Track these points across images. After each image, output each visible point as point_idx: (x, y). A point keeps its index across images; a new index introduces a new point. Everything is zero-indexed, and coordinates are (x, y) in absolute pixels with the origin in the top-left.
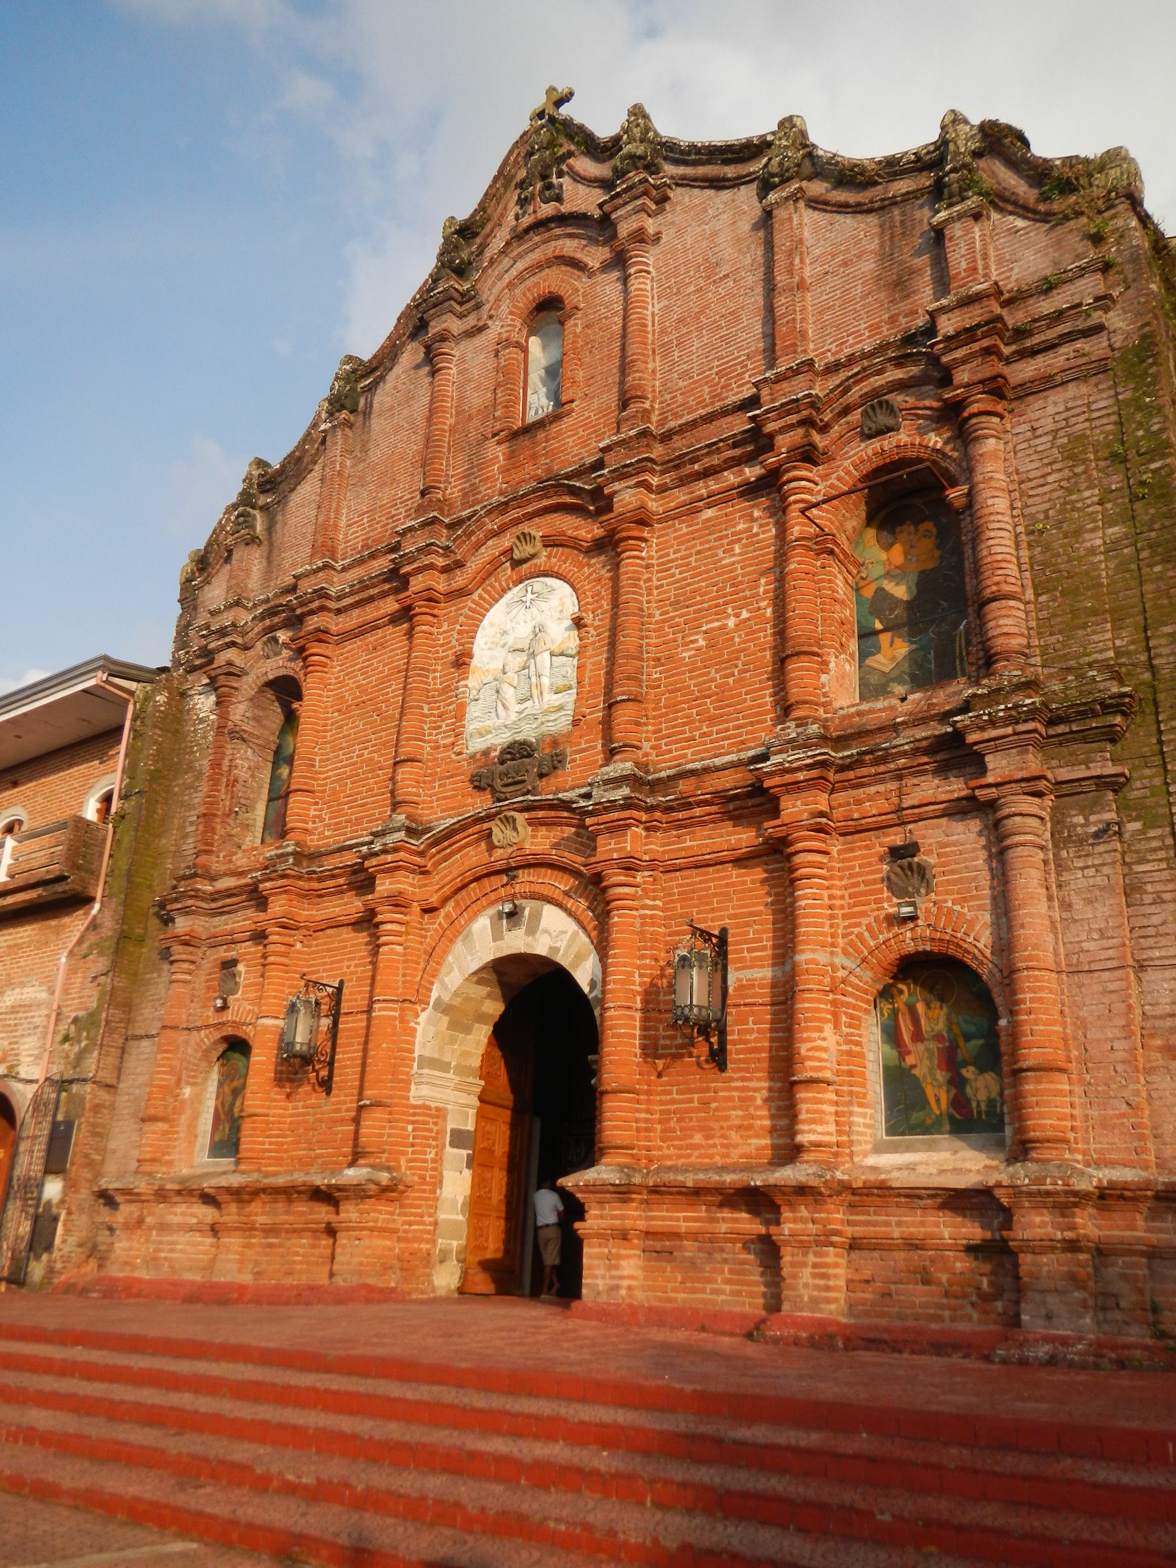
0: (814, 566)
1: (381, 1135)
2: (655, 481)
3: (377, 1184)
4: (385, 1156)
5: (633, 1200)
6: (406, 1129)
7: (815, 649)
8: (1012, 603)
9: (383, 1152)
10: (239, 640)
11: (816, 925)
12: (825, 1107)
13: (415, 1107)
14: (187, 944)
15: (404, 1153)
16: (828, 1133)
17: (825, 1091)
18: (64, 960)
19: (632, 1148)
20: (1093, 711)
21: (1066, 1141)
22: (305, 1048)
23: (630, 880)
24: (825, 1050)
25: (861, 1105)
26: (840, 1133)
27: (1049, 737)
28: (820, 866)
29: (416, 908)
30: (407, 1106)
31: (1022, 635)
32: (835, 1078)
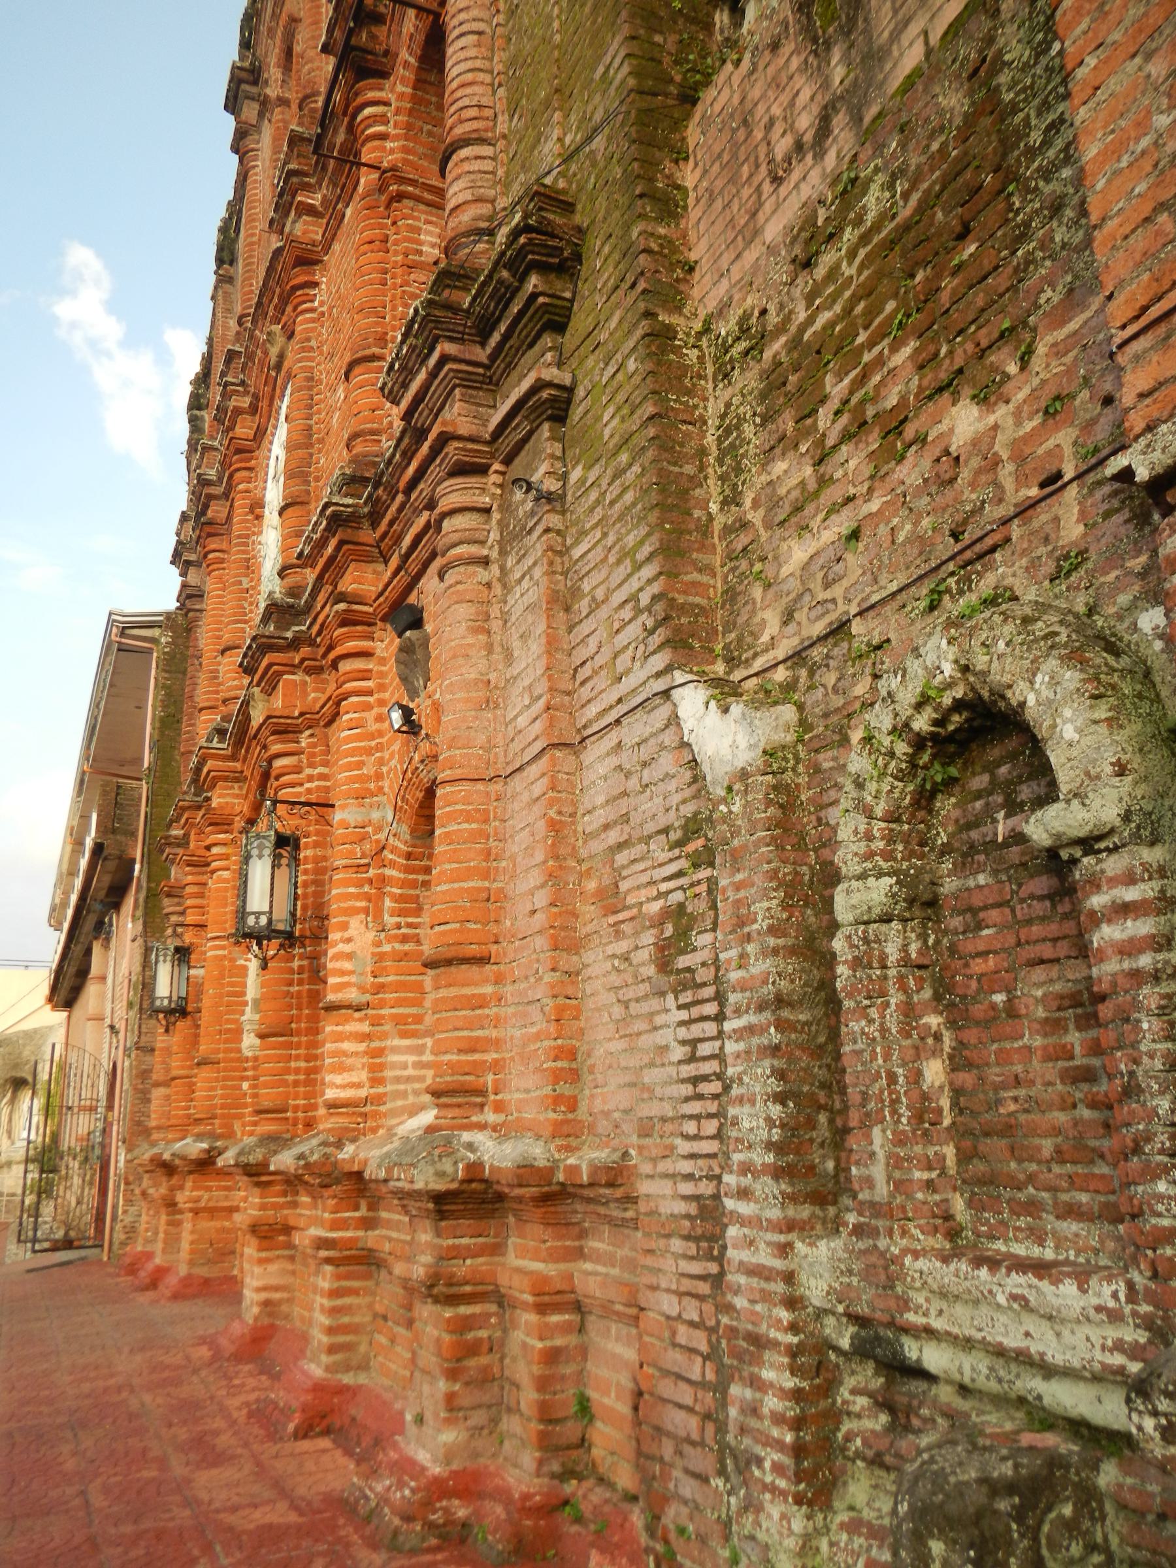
0: (382, 227)
1: (211, 1098)
2: (316, 200)
3: (183, 1158)
4: (217, 1121)
5: (269, 1183)
6: (240, 1088)
7: (376, 350)
8: (464, 152)
9: (214, 1117)
10: (193, 557)
11: (349, 767)
12: (347, 1046)
13: (247, 1059)
14: (169, 895)
15: (241, 1116)
16: (358, 1086)
17: (347, 1020)
18: (130, 925)
19: (286, 1111)
20: (501, 282)
21: (482, 1092)
22: (166, 1002)
23: (291, 746)
24: (349, 956)
25: (404, 1035)
26: (376, 1081)
27: (493, 357)
28: (365, 675)
29: (239, 823)
30: (240, 1060)
31: (479, 200)
32: (367, 997)
